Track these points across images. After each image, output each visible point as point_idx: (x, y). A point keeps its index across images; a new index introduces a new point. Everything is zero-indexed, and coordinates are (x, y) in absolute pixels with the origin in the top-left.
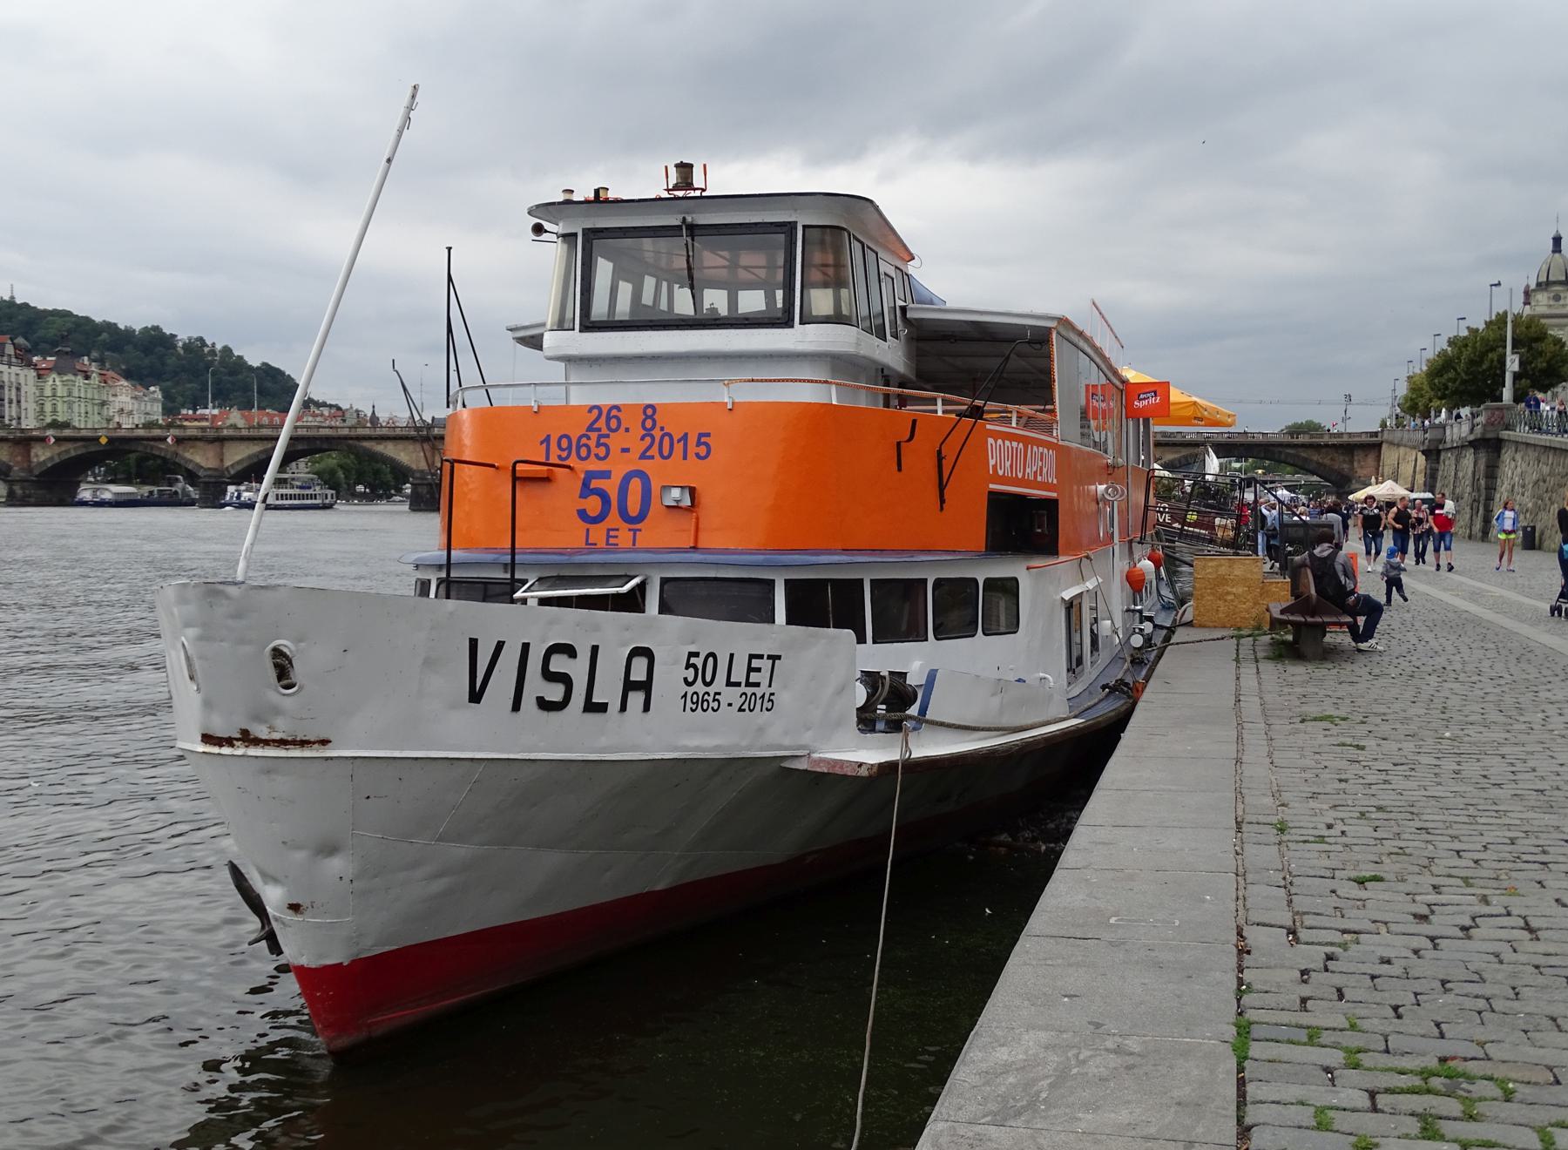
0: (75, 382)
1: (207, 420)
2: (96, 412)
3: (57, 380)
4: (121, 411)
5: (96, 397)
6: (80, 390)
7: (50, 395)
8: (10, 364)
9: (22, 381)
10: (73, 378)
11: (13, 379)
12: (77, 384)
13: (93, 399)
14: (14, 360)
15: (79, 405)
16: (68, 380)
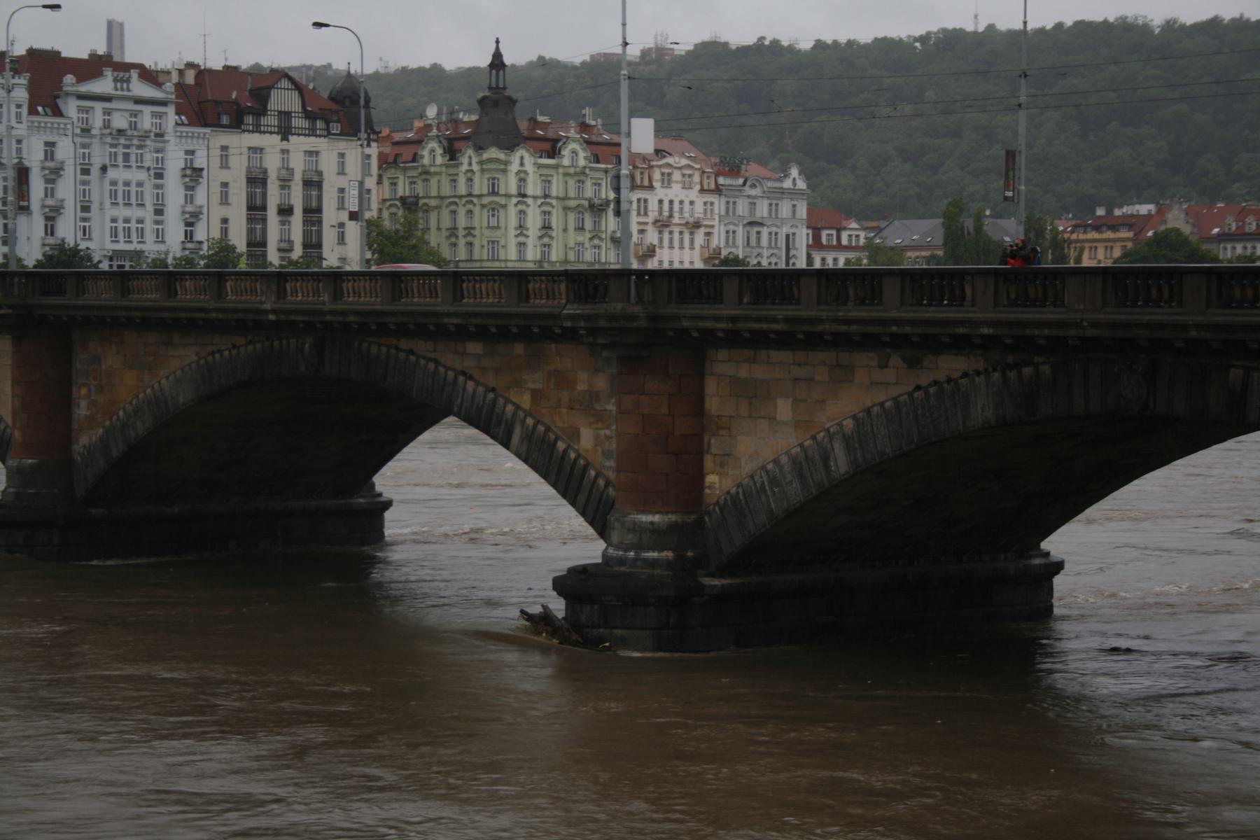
0: (507, 163)
1: (1130, 227)
2: (571, 226)
3: (474, 160)
4: (662, 224)
5: (572, 194)
6: (470, 180)
7: (539, 192)
8: (285, 132)
9: (328, 164)
10: (502, 156)
11: (298, 163)
12: (514, 167)
13: (566, 198)
14: (298, 122)
15: (470, 212)
16: (491, 160)
